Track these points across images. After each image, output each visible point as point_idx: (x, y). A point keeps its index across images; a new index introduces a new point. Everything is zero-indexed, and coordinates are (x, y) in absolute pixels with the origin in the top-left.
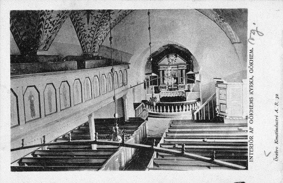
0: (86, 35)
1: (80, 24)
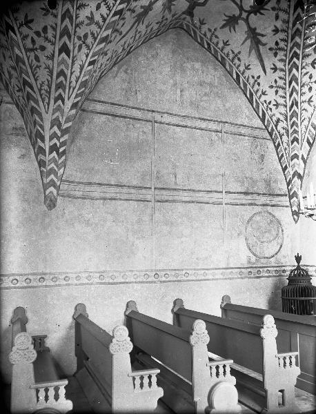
0: (270, 103)
1: (252, 81)
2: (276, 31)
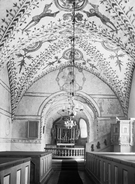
0: (16, 82)
2: (30, 65)
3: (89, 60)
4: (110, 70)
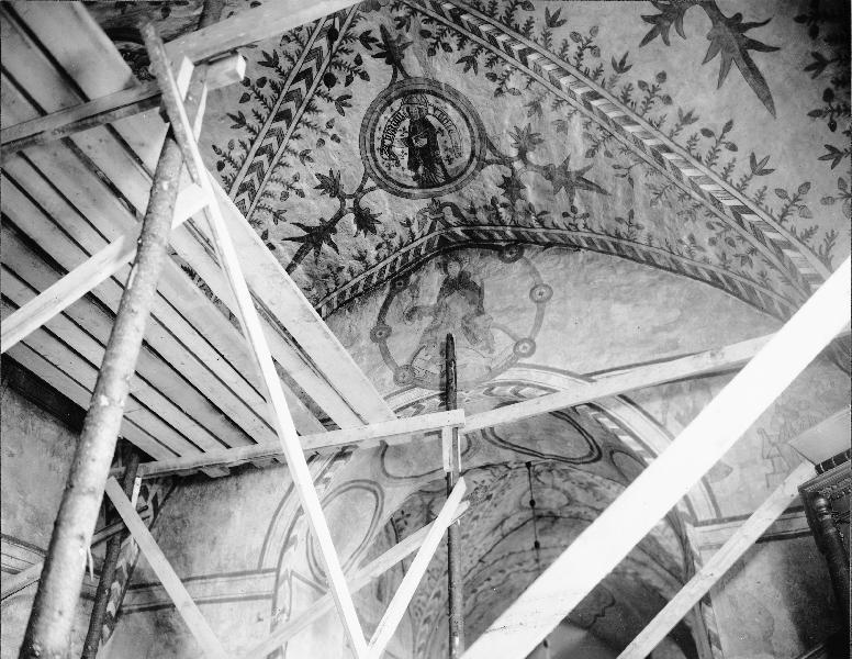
3: (527, 141)
4: (683, 138)
